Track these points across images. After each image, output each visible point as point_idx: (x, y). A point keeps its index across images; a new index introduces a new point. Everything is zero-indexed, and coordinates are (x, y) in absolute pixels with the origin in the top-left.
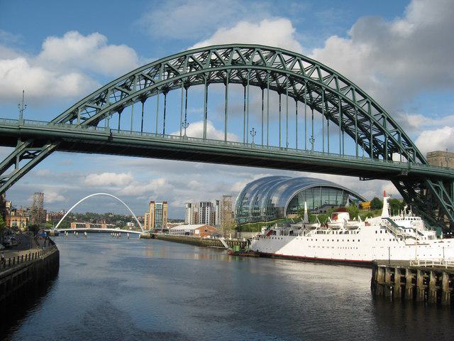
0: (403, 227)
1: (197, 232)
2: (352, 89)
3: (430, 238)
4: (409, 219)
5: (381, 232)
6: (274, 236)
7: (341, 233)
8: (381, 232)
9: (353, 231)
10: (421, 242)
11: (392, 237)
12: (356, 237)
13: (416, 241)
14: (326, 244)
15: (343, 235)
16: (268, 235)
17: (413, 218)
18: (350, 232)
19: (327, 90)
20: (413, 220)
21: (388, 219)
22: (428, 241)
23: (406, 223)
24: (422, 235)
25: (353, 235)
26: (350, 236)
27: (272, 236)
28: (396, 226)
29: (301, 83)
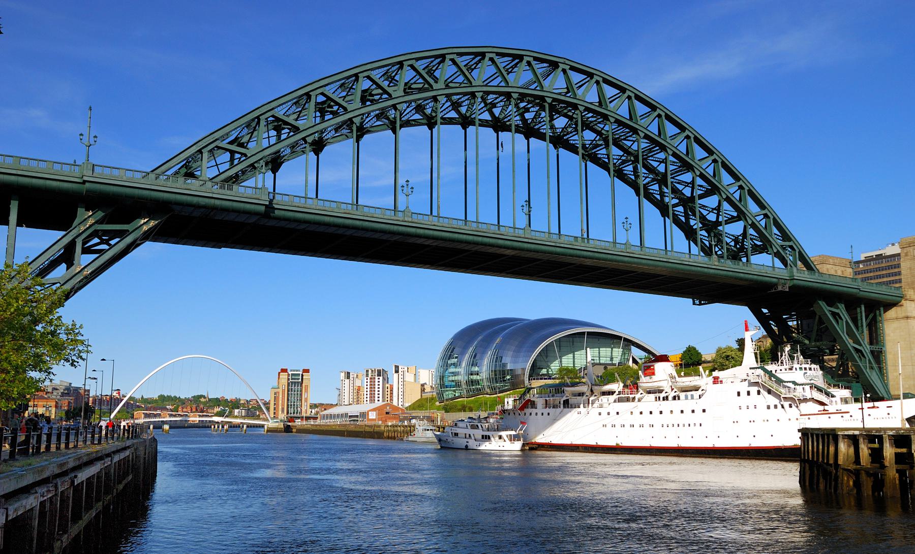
0: (795, 383)
1: (373, 415)
2: (659, 116)
3: (845, 401)
5: (749, 393)
6: (534, 411)
8: (749, 393)
9: (689, 394)
11: (772, 400)
12: (697, 405)
13: (821, 408)
14: (637, 419)
15: (670, 404)
17: (807, 366)
18: (682, 395)
19: (617, 121)
22: (844, 407)
23: (798, 376)
24: (833, 396)
25: (690, 401)
26: (685, 403)
27: (528, 411)
28: (779, 381)
29: (566, 116)
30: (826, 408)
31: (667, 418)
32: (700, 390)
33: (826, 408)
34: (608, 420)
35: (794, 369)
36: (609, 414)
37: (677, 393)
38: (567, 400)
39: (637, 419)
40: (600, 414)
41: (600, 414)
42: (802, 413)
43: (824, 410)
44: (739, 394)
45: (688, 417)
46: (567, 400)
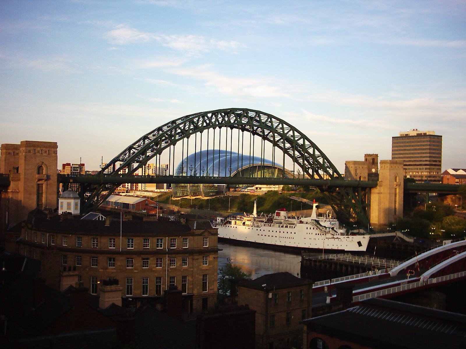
4: (329, 221)
7: (282, 227)
9: (291, 225)
10: (335, 237)
11: (318, 231)
12: (293, 230)
13: (332, 236)
16: (225, 224)
18: (289, 226)
20: (332, 222)
21: (315, 220)
22: (339, 237)
24: (337, 232)
25: (291, 229)
26: (289, 230)
27: (227, 225)
30: (334, 236)
31: (282, 234)
32: (295, 225)
33: (334, 236)
34: (261, 233)
35: (327, 221)
36: (261, 230)
37: (286, 225)
38: (245, 222)
39: (271, 234)
40: (257, 230)
41: (257, 230)
42: (327, 237)
43: (333, 237)
44: (307, 228)
45: (289, 235)
46: (245, 222)
